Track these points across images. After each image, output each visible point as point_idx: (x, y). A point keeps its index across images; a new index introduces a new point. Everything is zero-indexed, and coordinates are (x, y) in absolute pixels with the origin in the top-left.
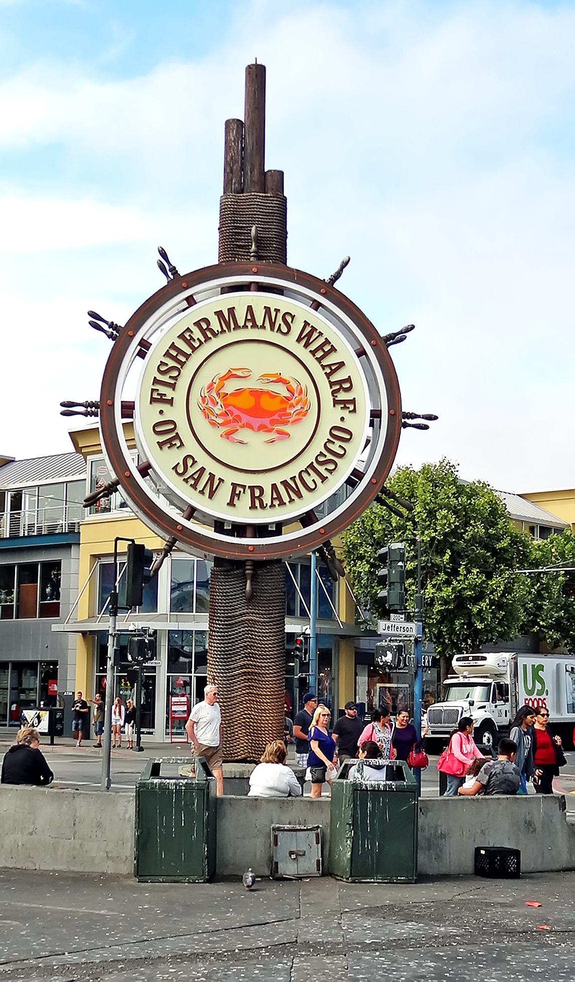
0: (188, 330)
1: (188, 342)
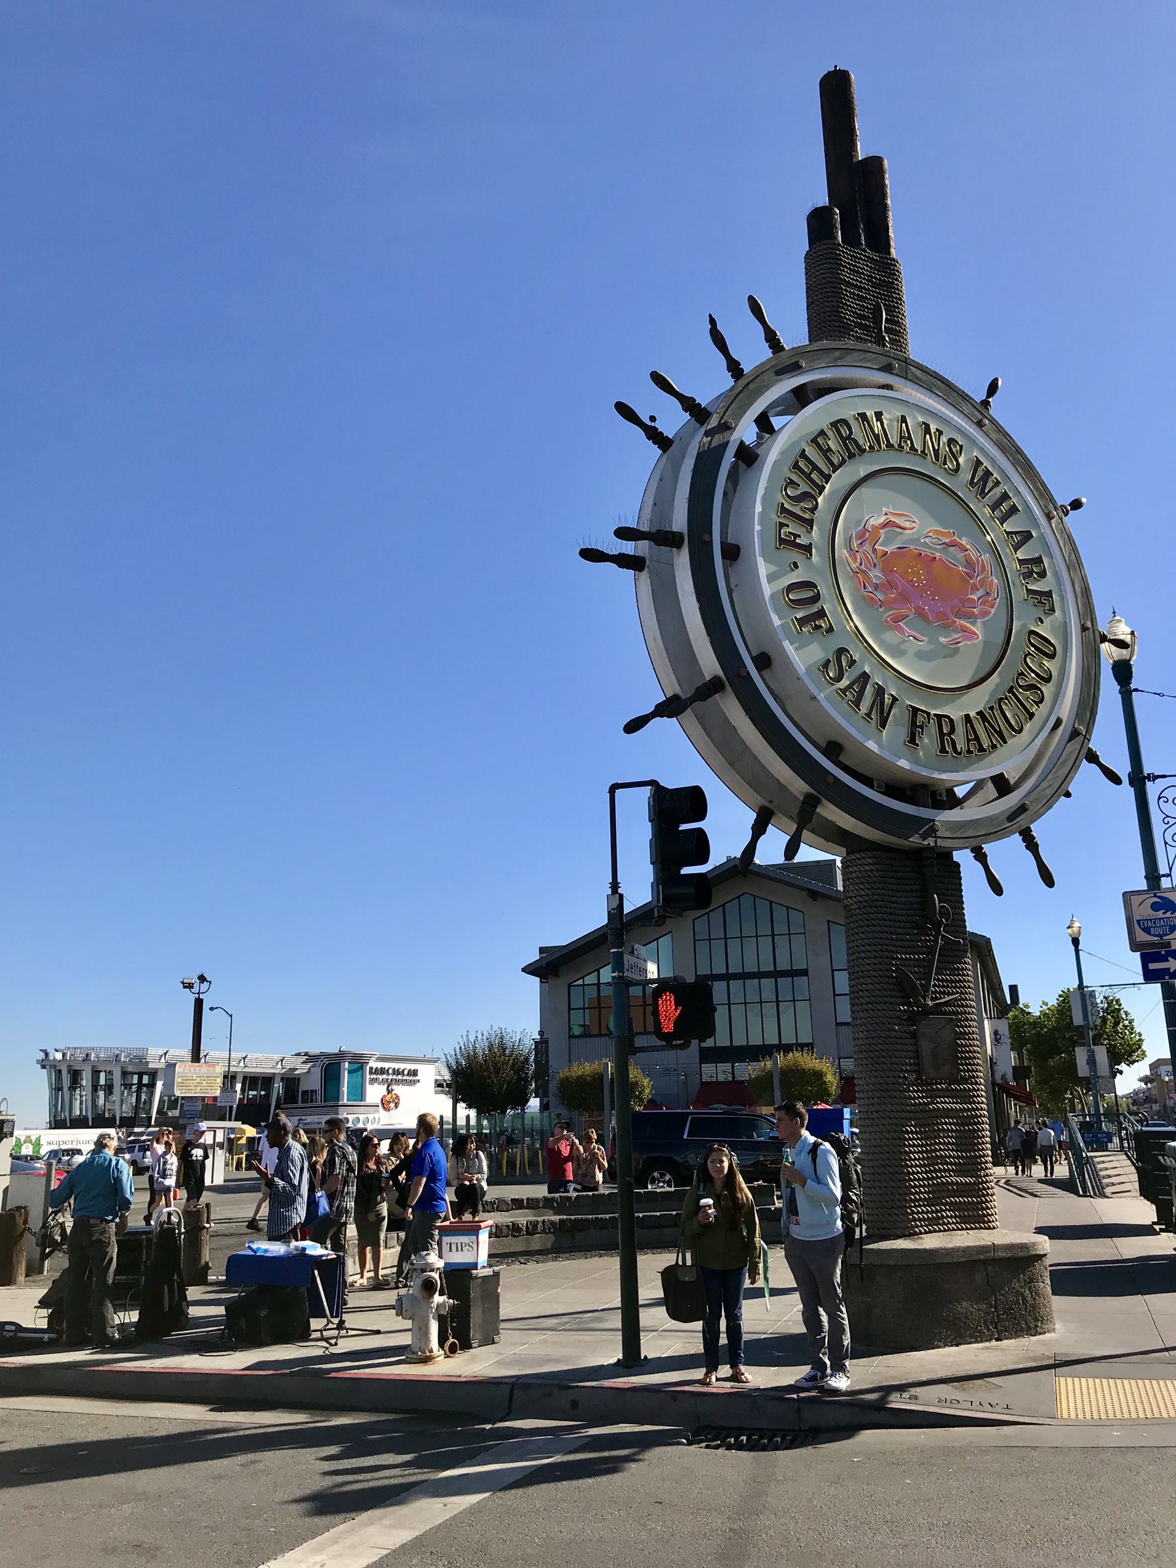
0: (822, 433)
1: (826, 452)
